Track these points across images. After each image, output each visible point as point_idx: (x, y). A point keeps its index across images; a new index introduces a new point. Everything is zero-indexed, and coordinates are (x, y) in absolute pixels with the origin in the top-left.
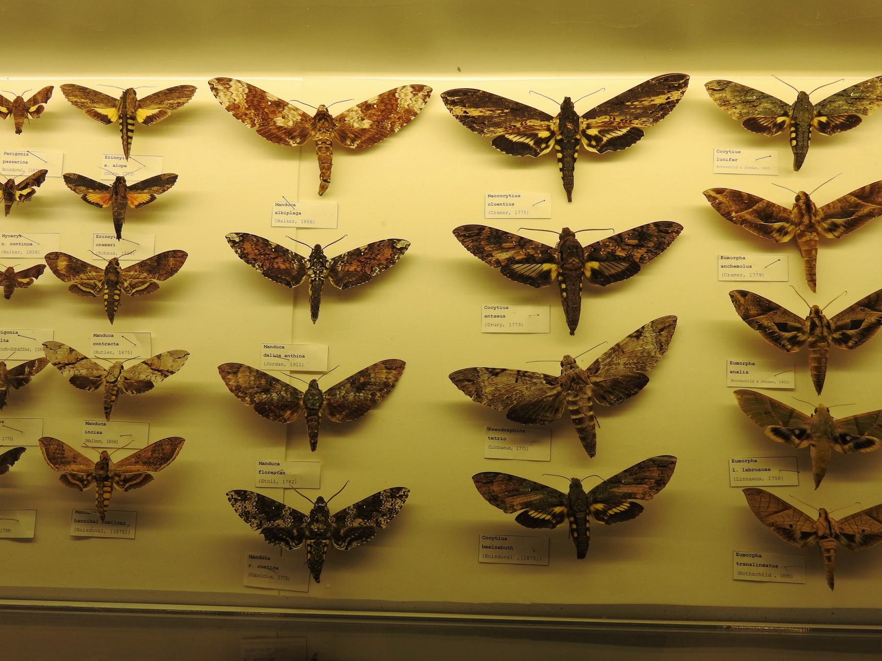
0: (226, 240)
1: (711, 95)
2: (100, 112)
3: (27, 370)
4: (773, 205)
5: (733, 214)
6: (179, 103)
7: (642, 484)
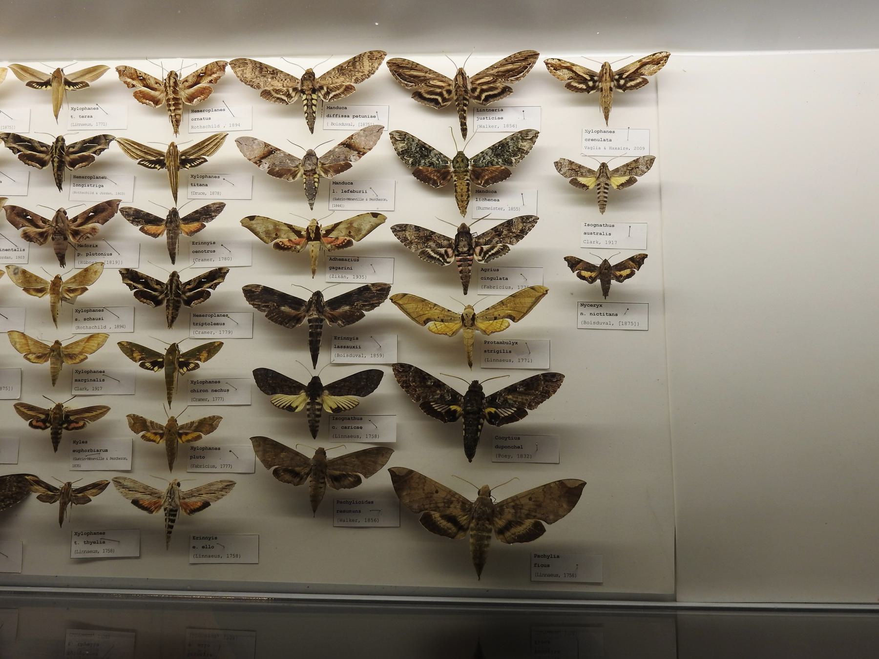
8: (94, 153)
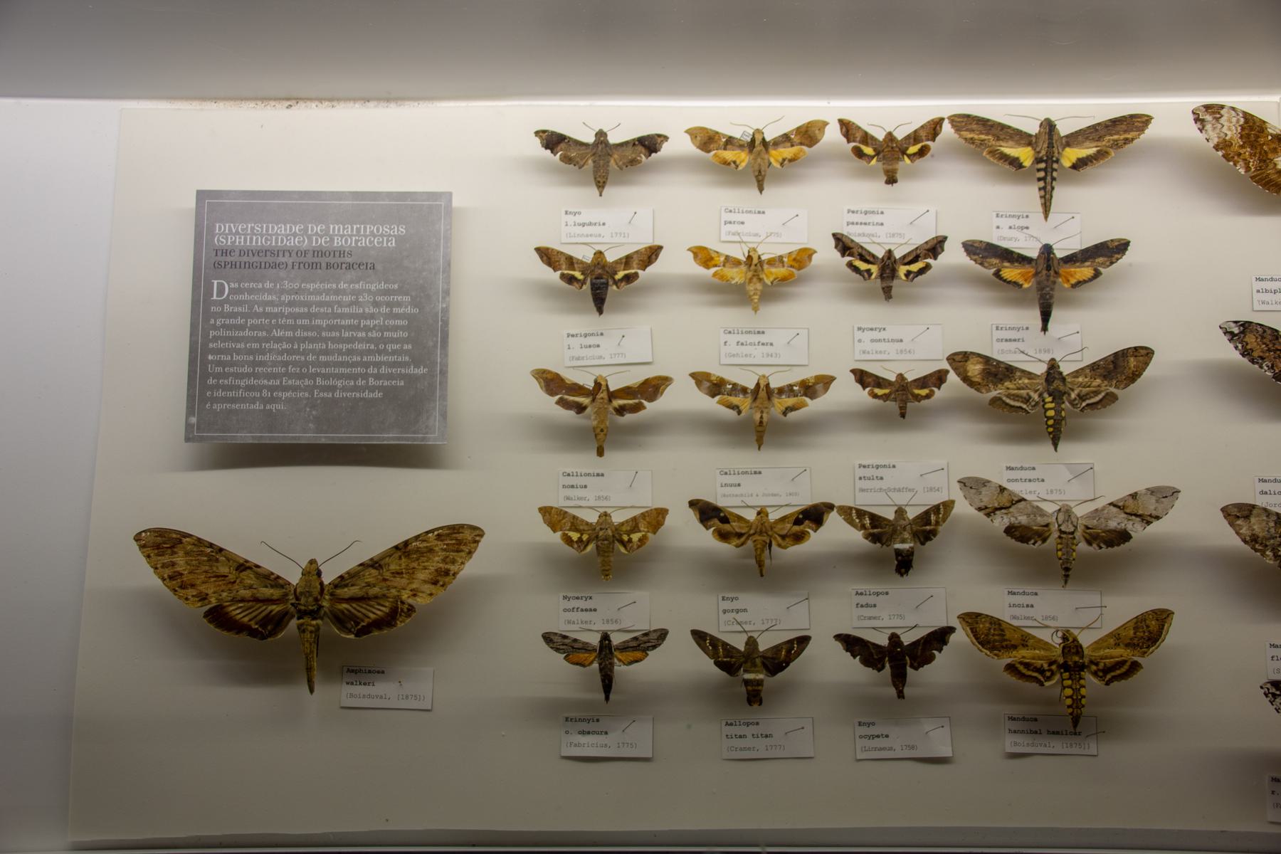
0: (1221, 332)
2: (1008, 153)
3: (933, 518)
6: (1127, 139)
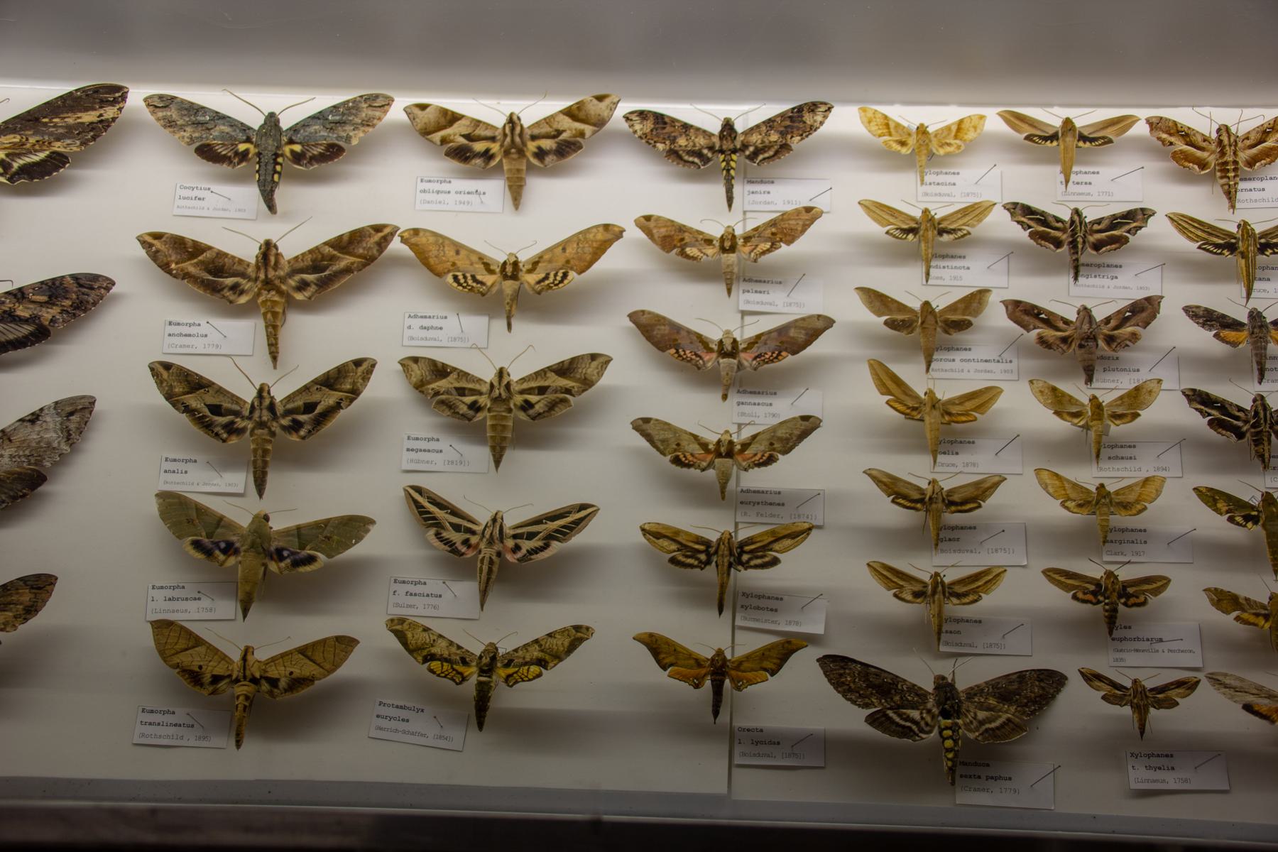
1: (153, 113)
4: (226, 255)
5: (173, 266)
7: (4, 611)
8: (1128, 232)
